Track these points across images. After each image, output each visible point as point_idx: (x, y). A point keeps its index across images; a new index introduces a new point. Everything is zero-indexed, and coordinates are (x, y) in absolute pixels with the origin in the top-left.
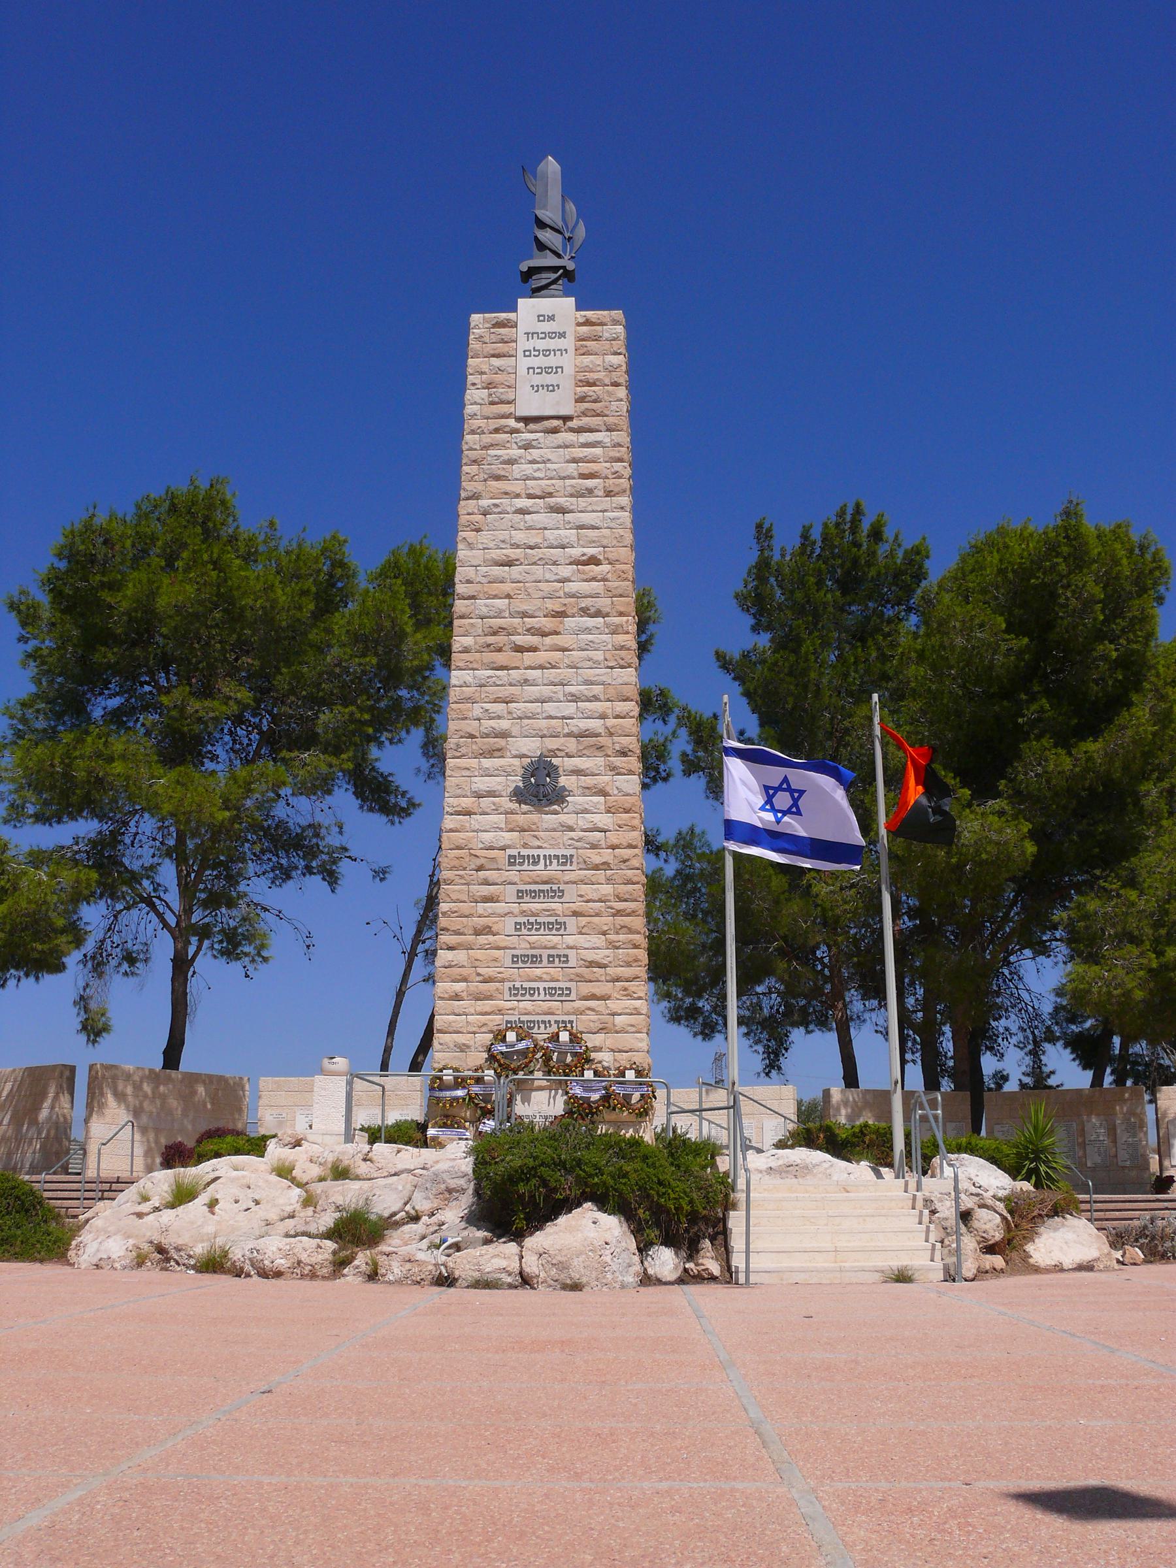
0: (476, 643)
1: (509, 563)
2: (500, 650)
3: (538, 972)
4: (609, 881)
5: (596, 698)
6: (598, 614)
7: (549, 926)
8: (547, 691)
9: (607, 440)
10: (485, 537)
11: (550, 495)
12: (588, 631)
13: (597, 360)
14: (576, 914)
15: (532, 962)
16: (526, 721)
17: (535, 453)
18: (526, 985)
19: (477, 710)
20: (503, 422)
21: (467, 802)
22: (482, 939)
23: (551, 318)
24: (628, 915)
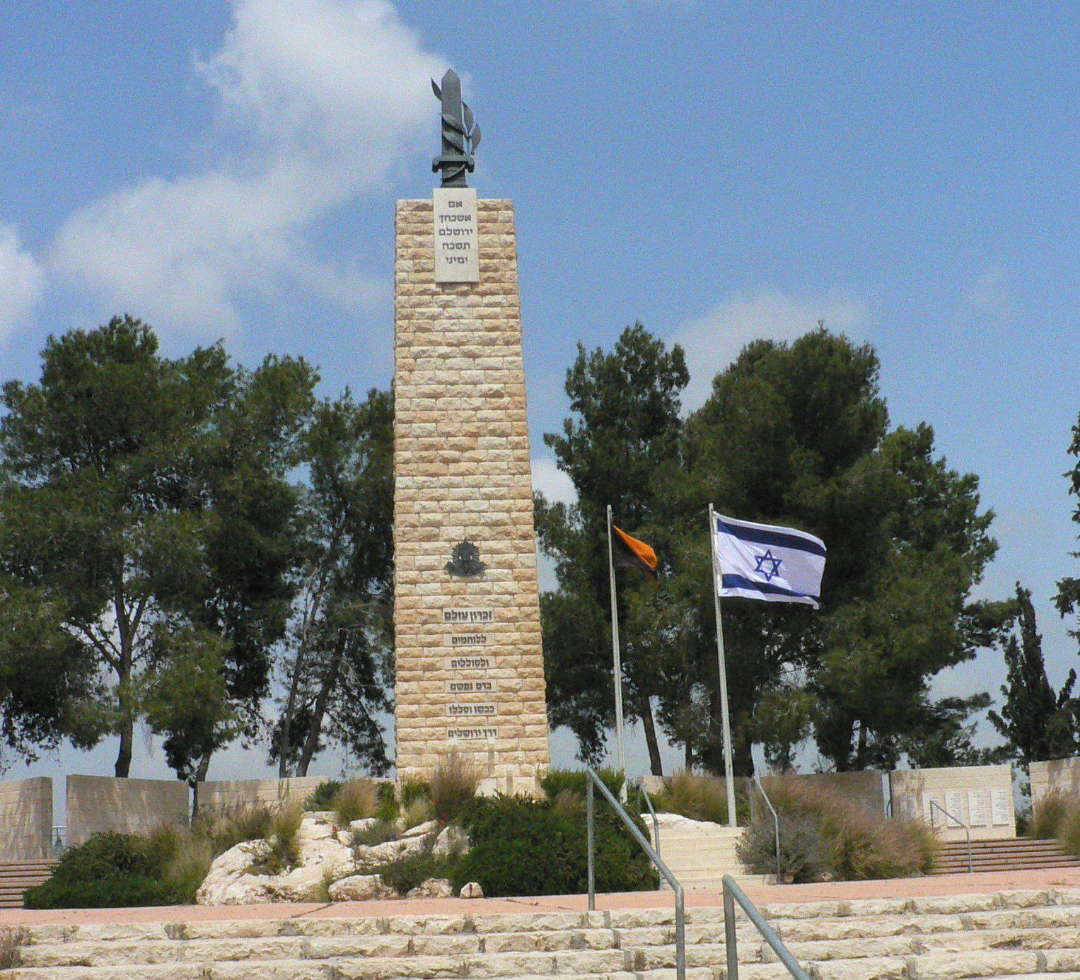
0: (413, 456)
1: (436, 396)
2: (431, 462)
3: (470, 696)
4: (518, 629)
5: (502, 498)
6: (503, 434)
7: (476, 663)
8: (466, 491)
9: (505, 301)
10: (416, 376)
11: (464, 344)
12: (495, 447)
13: (495, 238)
14: (495, 654)
15: (466, 689)
16: (453, 515)
17: (450, 311)
18: (462, 705)
19: (417, 506)
20: (426, 286)
21: (413, 574)
22: (428, 674)
23: (460, 204)
24: (532, 654)
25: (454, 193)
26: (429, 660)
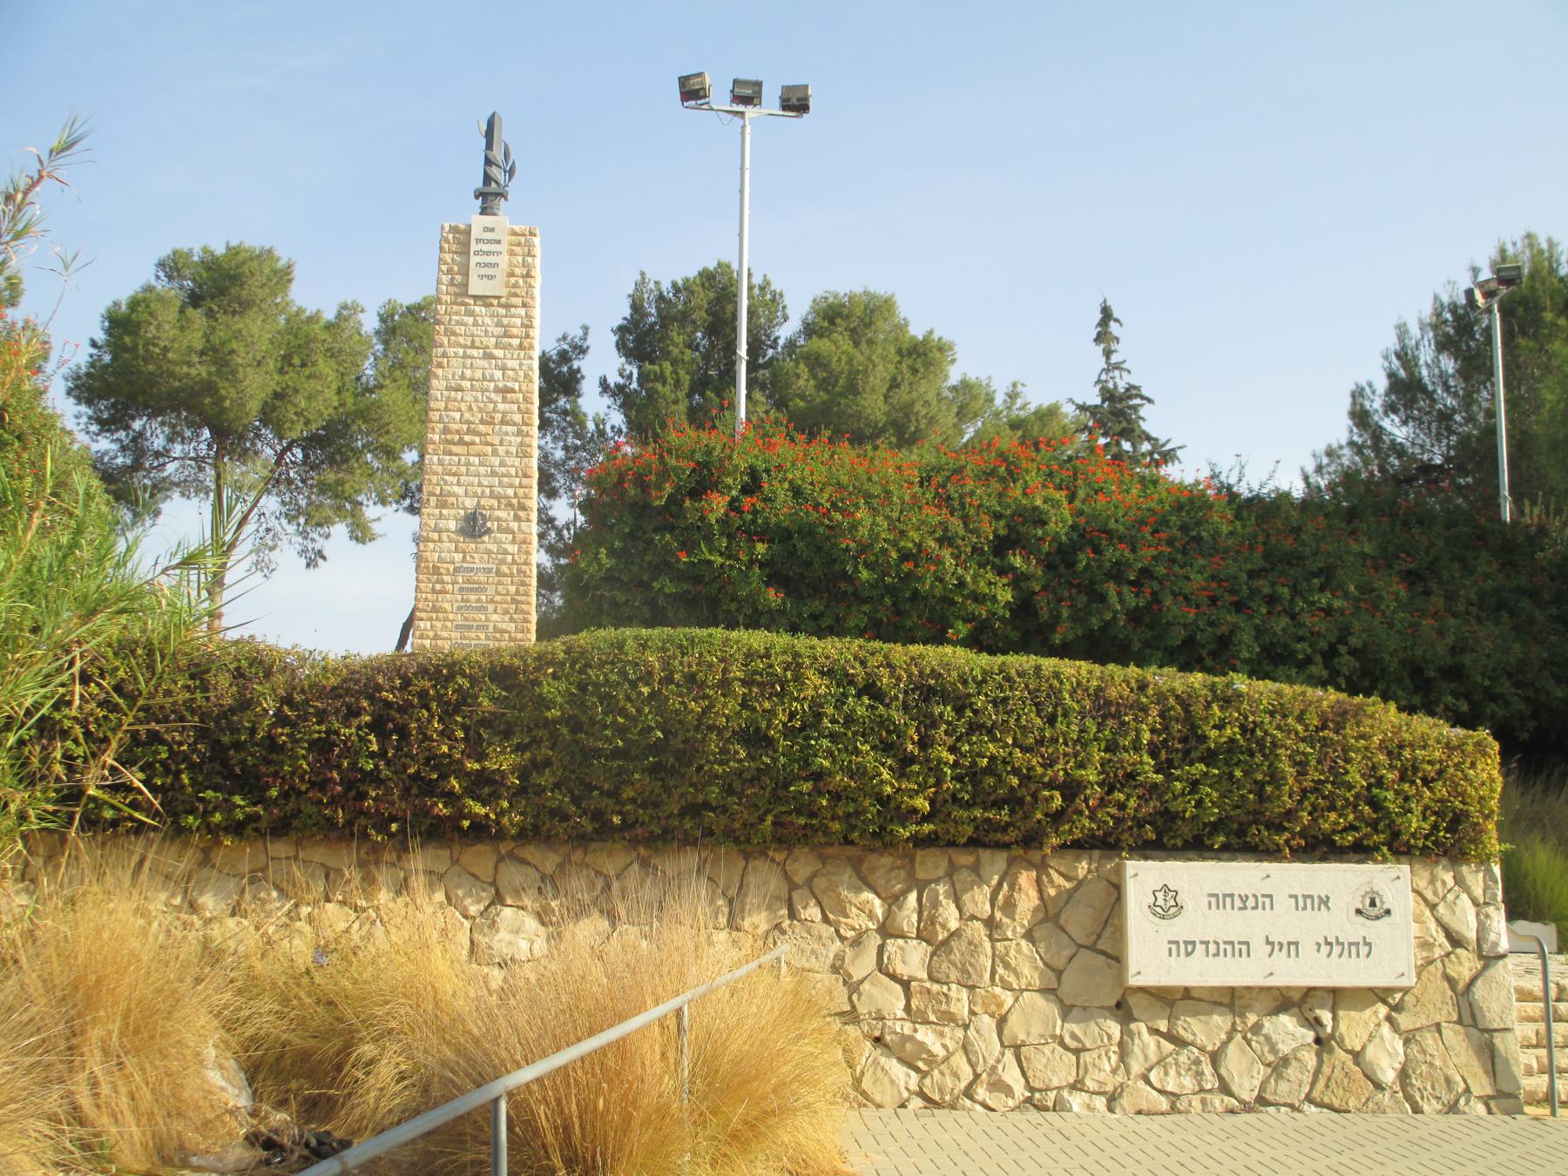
23: (492, 230)
25: (488, 220)
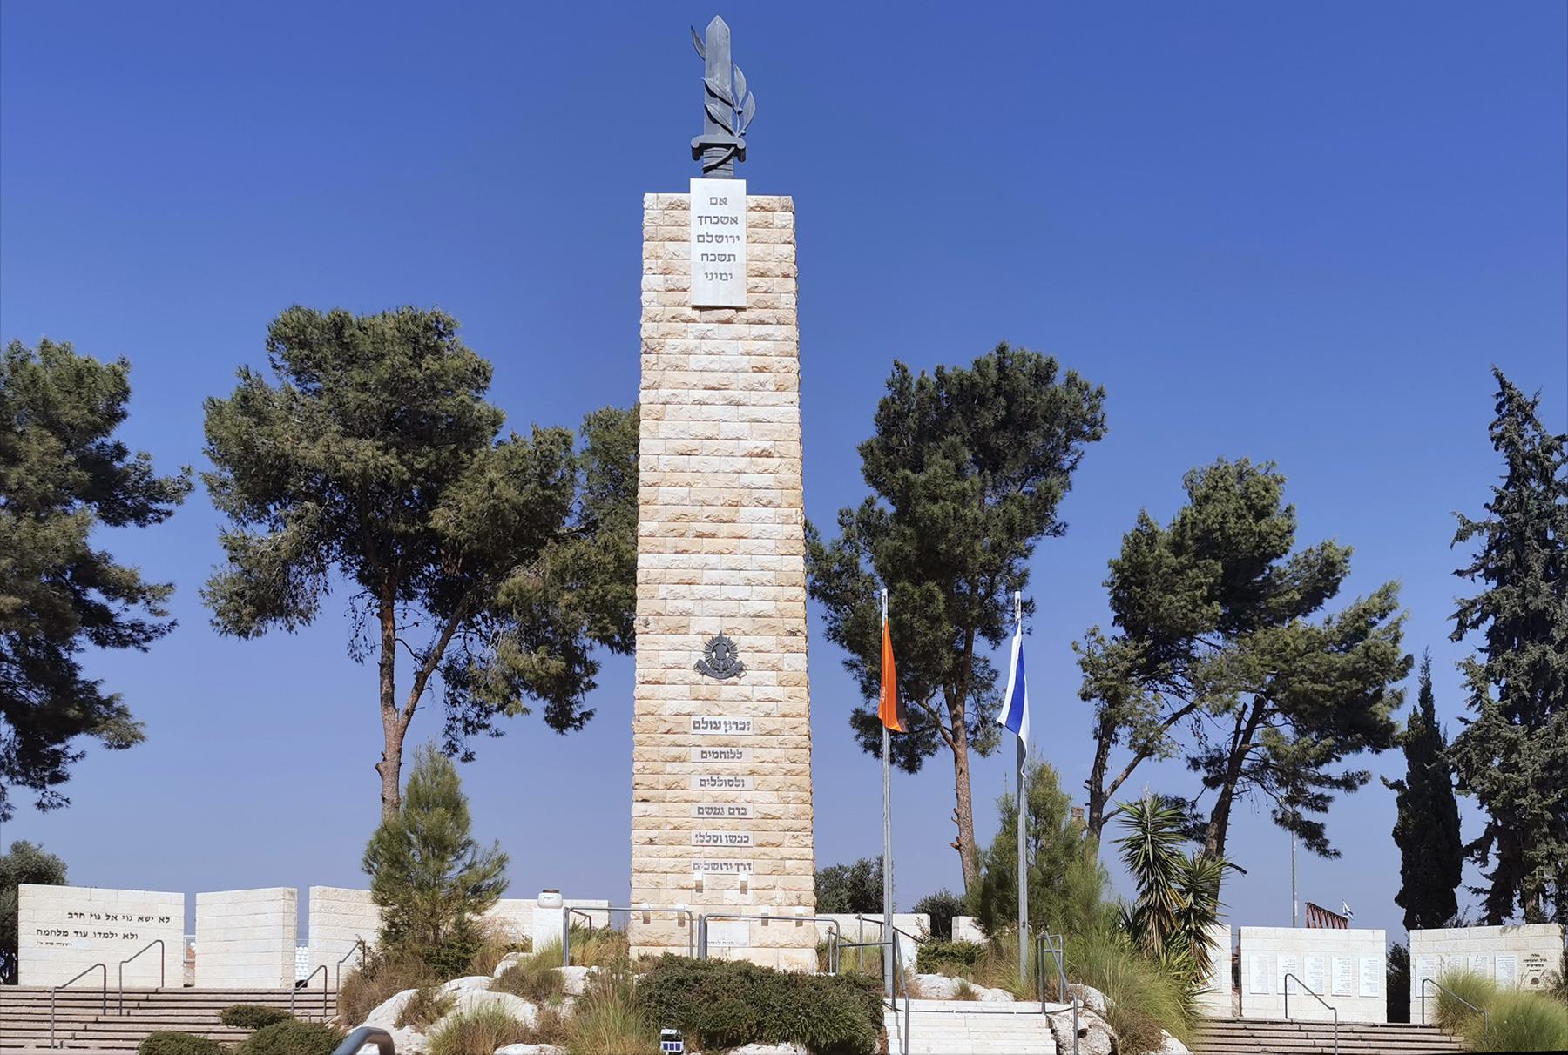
3: (721, 822)
7: (730, 783)
8: (725, 575)
14: (752, 773)
16: (706, 602)
17: (709, 345)
18: (711, 833)
19: (663, 591)
21: (654, 674)
23: (724, 201)
26: (671, 778)
